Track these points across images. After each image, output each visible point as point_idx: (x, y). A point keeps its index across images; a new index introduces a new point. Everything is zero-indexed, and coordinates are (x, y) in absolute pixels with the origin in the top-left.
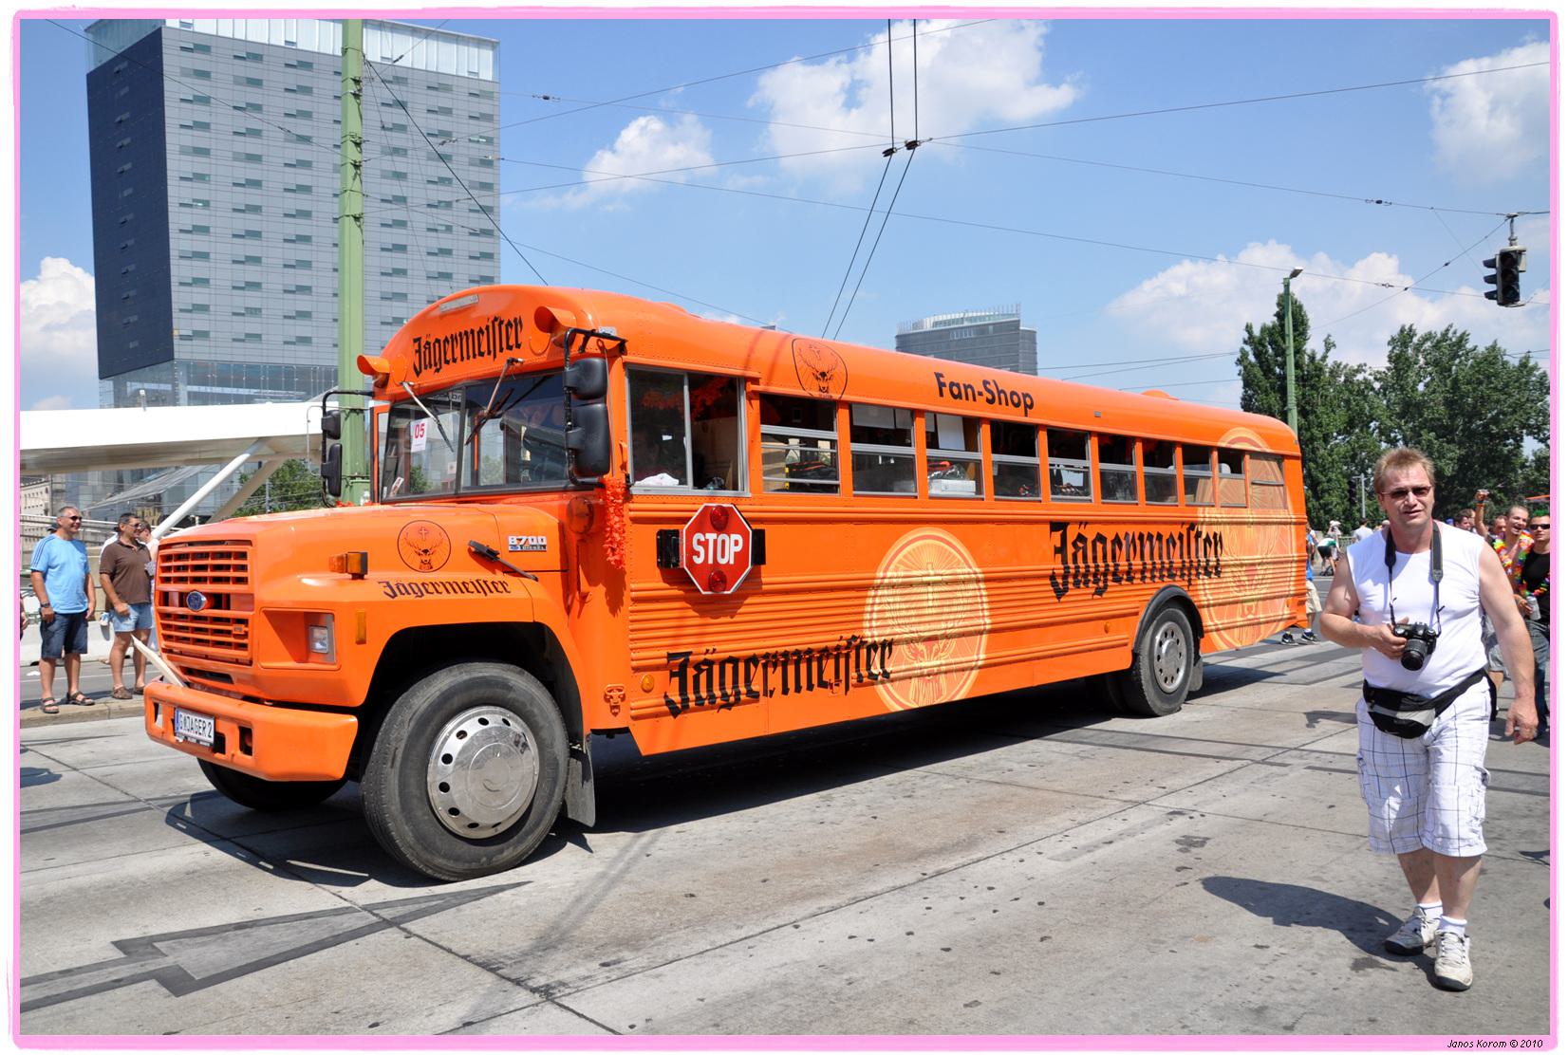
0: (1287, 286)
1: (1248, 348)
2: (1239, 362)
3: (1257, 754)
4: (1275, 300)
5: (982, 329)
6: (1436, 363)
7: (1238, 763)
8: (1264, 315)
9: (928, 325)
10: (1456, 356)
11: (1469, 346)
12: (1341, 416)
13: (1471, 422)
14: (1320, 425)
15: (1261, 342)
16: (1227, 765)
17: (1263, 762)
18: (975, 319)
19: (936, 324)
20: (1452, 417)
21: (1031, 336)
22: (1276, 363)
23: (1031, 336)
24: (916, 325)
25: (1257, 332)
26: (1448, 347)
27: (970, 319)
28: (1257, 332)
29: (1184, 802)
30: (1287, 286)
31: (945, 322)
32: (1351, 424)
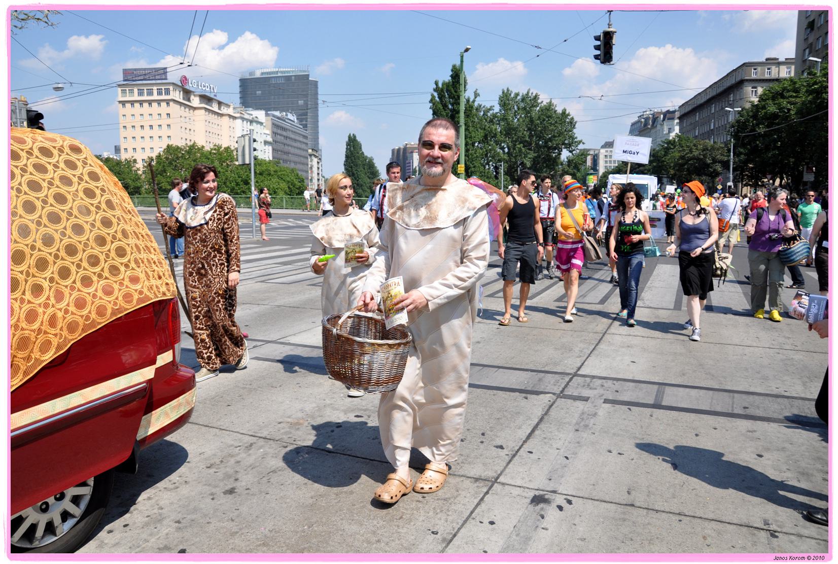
0: (462, 57)
1: (436, 94)
2: (431, 101)
3: (552, 384)
4: (451, 68)
5: (288, 78)
6: (525, 108)
7: (546, 399)
8: (446, 77)
9: (258, 74)
10: (533, 106)
11: (539, 101)
12: (481, 133)
13: (539, 140)
14: (471, 137)
15: (442, 90)
16: (537, 405)
17: (562, 395)
18: (284, 72)
19: (262, 74)
20: (531, 136)
21: (315, 84)
22: (449, 101)
23: (315, 84)
24: (251, 74)
25: (440, 85)
26: (530, 101)
27: (282, 72)
28: (440, 85)
29: (539, 482)
30: (462, 57)
31: (268, 73)
32: (486, 137)
